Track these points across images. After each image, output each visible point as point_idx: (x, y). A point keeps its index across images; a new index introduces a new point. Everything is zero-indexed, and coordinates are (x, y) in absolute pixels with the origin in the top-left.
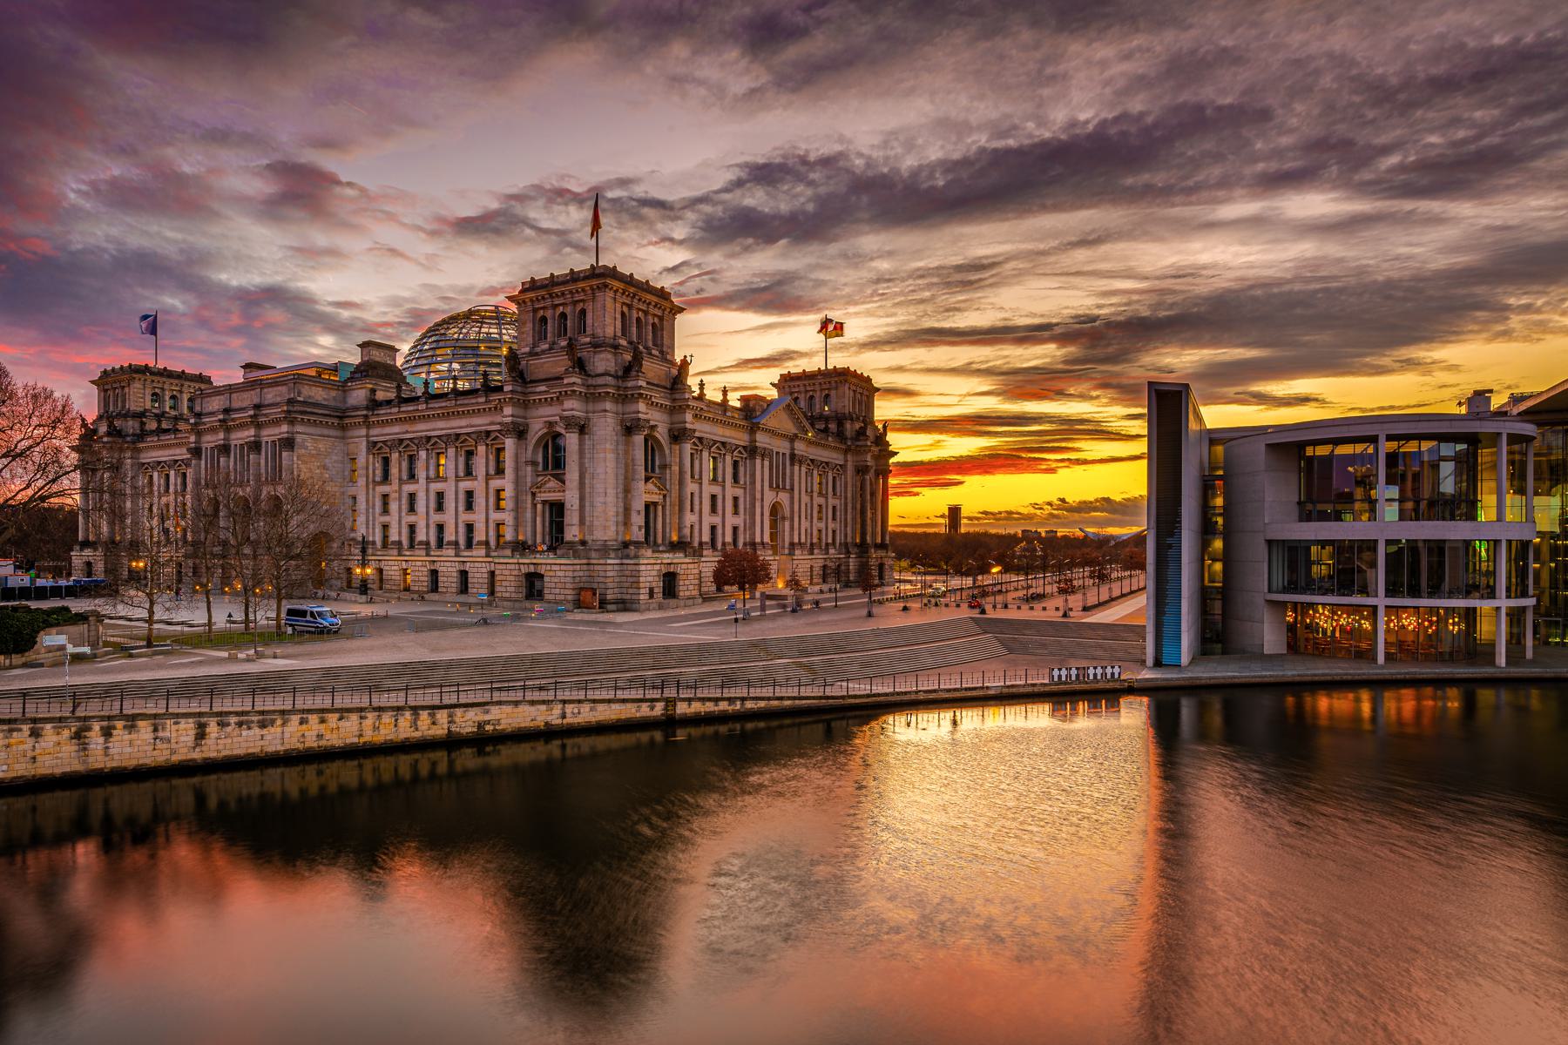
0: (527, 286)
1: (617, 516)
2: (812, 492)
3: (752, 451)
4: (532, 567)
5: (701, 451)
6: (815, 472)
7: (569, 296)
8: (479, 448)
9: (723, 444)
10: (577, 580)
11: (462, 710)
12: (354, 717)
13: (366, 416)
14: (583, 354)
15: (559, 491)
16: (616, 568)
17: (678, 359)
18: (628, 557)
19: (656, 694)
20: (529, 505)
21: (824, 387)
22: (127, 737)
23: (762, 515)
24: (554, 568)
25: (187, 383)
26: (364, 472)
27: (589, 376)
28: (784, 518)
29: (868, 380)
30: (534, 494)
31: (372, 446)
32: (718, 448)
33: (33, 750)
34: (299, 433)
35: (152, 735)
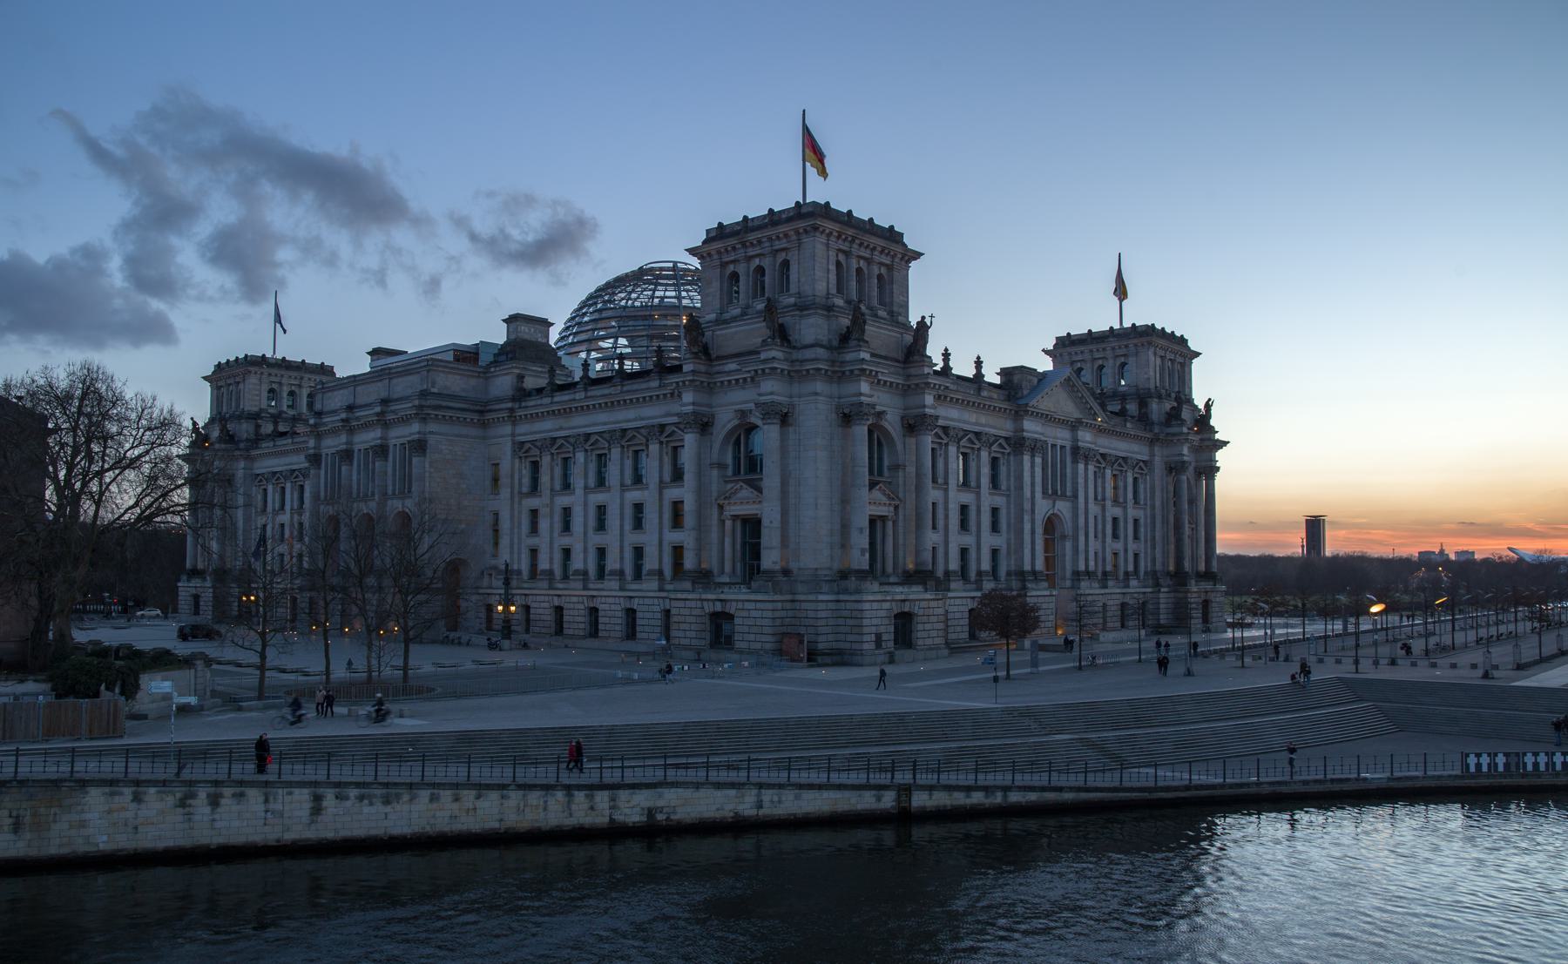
0: (713, 234)
2: (1104, 499)
3: (1018, 444)
4: (718, 604)
5: (947, 445)
6: (1108, 472)
7: (767, 244)
8: (651, 447)
9: (977, 434)
11: (627, 792)
12: (494, 795)
13: (512, 410)
14: (786, 320)
16: (831, 606)
17: (914, 320)
18: (846, 591)
19: (884, 778)
21: (1119, 352)
22: (235, 808)
23: (1033, 532)
25: (307, 376)
27: (794, 348)
28: (1064, 537)
29: (1182, 341)
30: (721, 507)
31: (520, 447)
32: (970, 441)
33: (136, 818)
34: (431, 433)
35: (262, 807)
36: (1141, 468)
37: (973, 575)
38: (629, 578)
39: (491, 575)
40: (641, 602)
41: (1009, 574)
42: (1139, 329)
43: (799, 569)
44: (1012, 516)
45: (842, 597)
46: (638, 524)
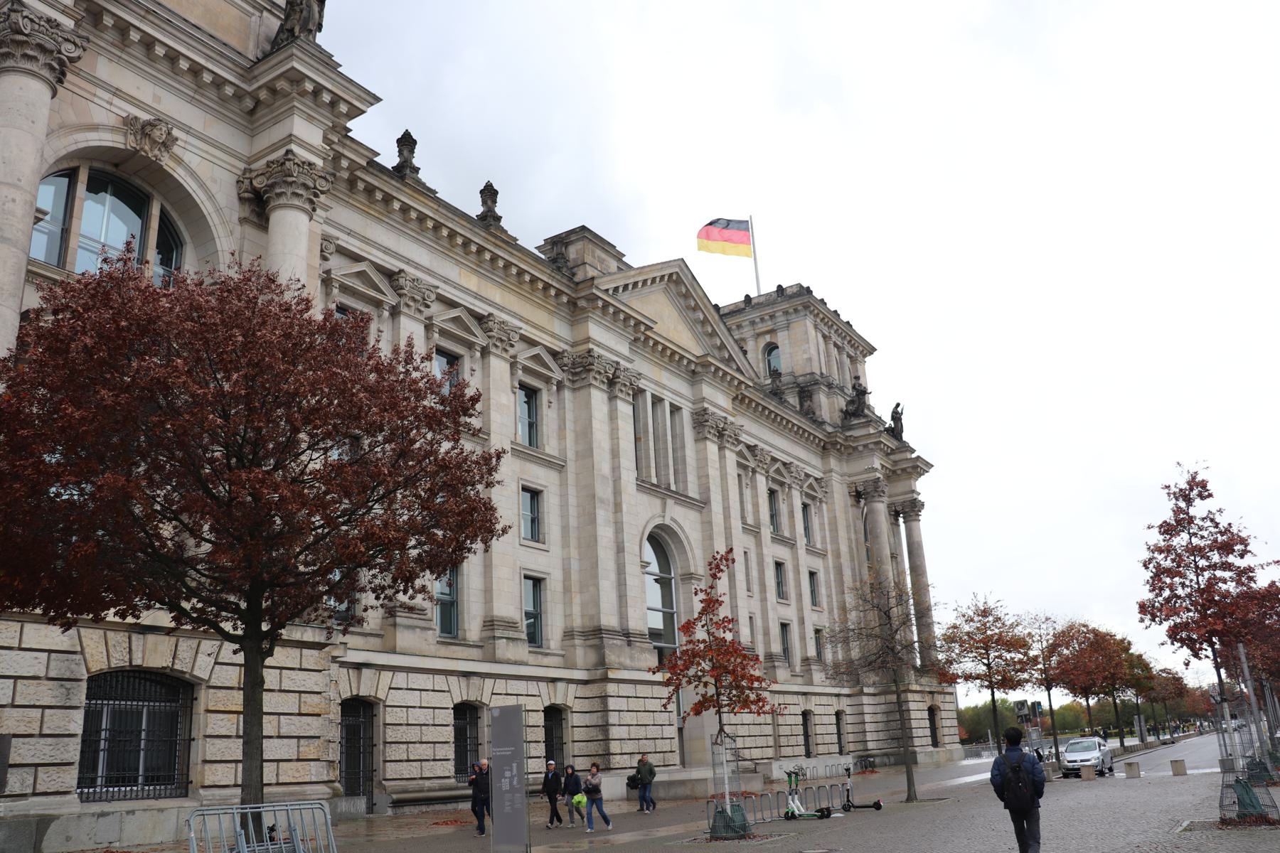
21: (762, 327)
28: (688, 577)
36: (811, 486)
37: (472, 628)
41: (569, 634)
42: (789, 292)
44: (573, 511)
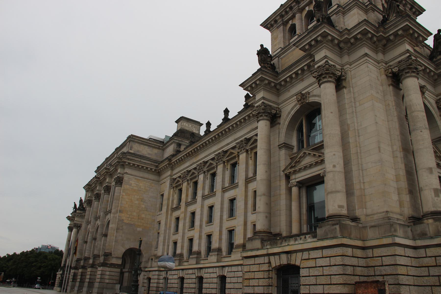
1: (398, 180)
4: (284, 257)
8: (241, 157)
10: (349, 270)
14: (333, 18)
15: (317, 164)
18: (423, 235)
20: (283, 191)
24: (314, 254)
26: (166, 202)
34: (126, 173)
38: (224, 254)
39: (152, 259)
40: (230, 270)
43: (367, 215)
45: (419, 243)
46: (232, 213)
